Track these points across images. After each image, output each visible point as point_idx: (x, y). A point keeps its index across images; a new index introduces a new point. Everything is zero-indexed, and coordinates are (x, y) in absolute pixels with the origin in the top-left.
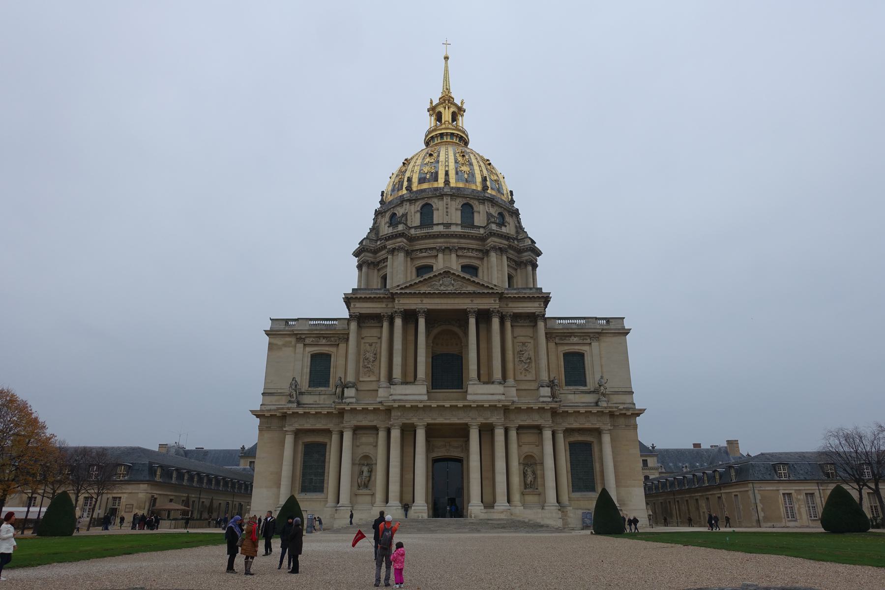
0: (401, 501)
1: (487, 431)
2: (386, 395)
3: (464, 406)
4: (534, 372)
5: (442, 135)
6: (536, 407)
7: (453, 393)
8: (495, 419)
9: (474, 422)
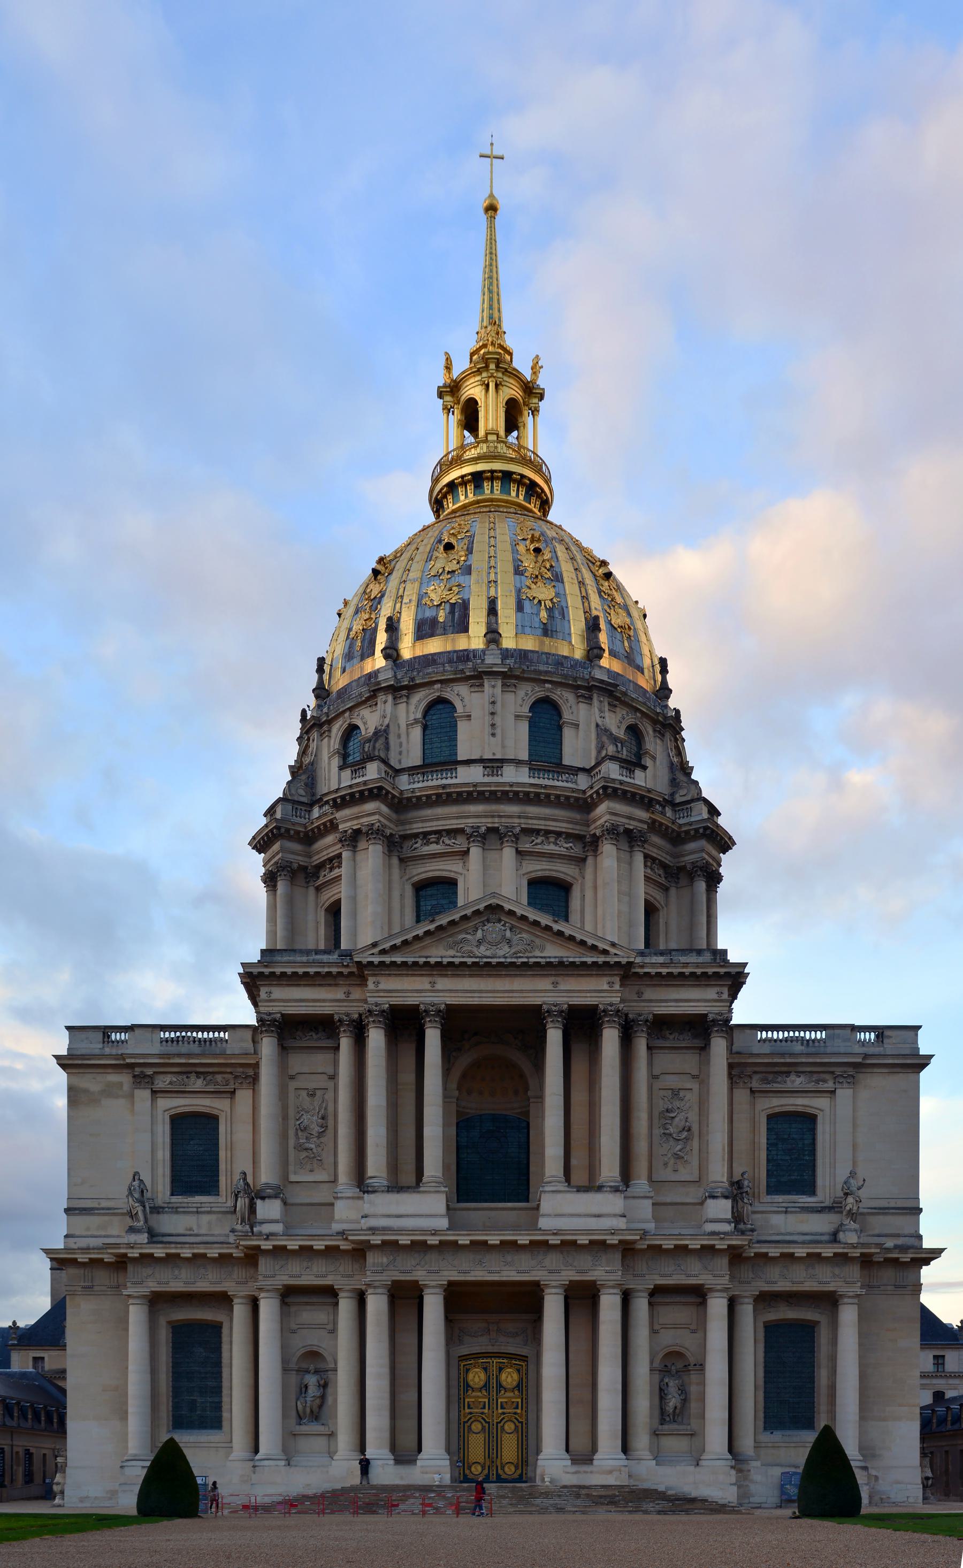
0: (393, 1448)
1: (582, 1298)
2: (354, 1215)
3: (532, 1243)
4: (695, 1163)
5: (477, 479)
6: (695, 1244)
7: (507, 1211)
8: (604, 1271)
9: (554, 1276)
